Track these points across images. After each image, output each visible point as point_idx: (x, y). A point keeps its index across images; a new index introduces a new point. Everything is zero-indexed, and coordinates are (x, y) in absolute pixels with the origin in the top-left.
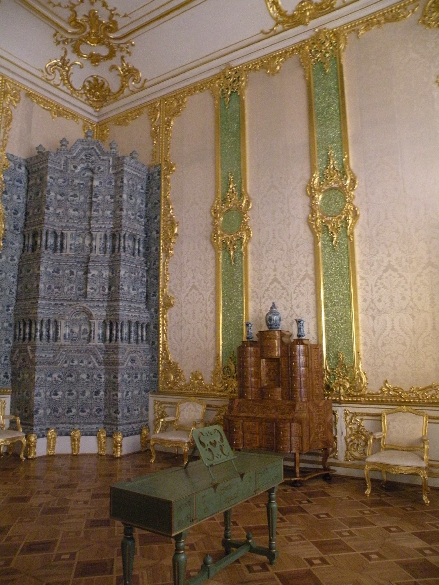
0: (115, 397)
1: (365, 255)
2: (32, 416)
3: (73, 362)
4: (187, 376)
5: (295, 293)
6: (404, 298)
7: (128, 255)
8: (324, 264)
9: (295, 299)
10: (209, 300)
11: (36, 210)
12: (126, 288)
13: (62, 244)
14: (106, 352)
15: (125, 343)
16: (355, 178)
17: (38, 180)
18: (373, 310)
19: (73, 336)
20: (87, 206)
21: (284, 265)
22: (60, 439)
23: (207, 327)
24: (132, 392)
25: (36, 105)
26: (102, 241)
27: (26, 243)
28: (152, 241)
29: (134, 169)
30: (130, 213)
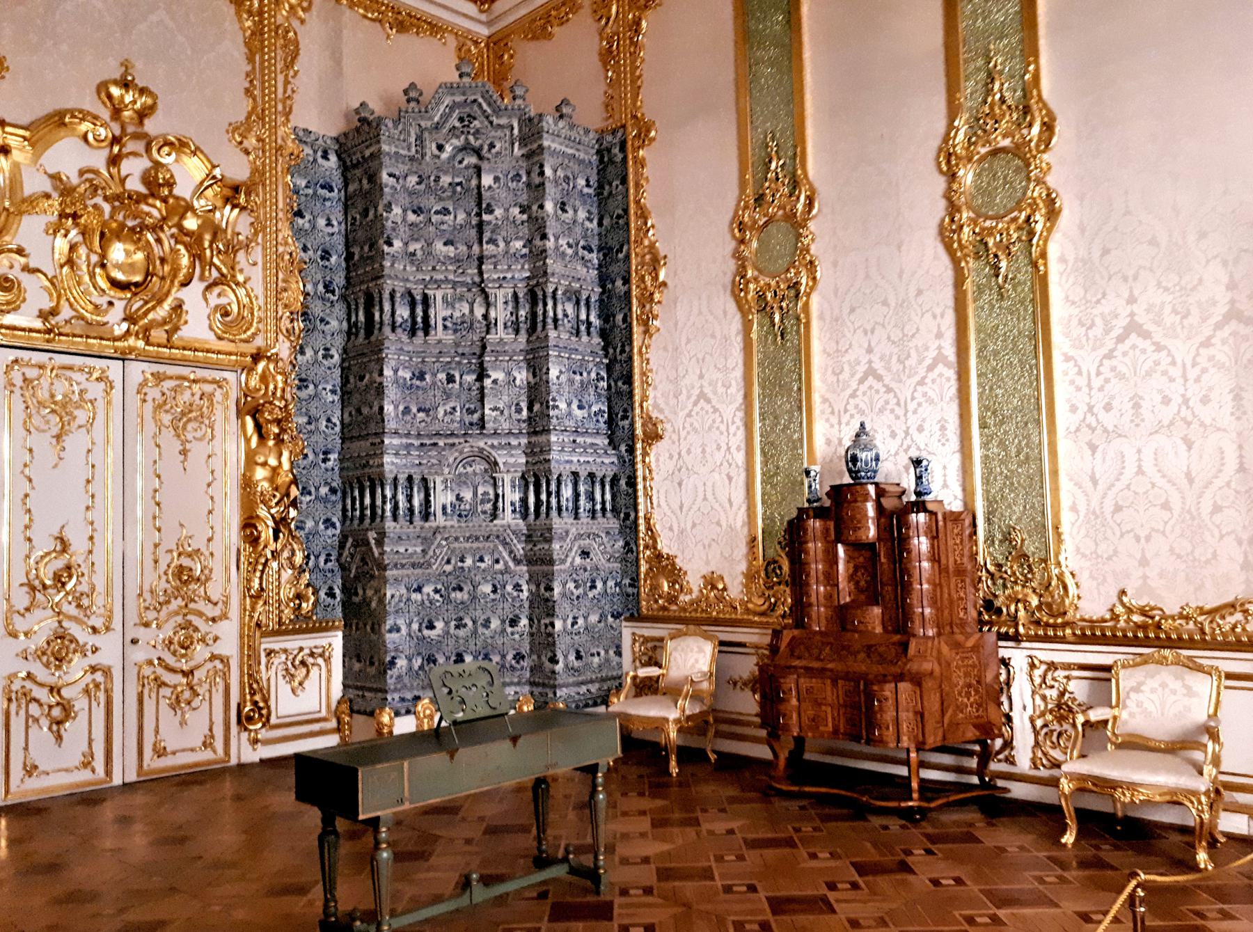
0: (550, 628)
1: (1073, 303)
2: (385, 672)
3: (462, 561)
4: (694, 582)
5: (913, 399)
6: (1166, 401)
7: (564, 336)
8: (978, 331)
9: (915, 412)
10: (733, 423)
11: (366, 248)
12: (563, 406)
13: (426, 318)
14: (529, 538)
15: (568, 519)
16: (1053, 118)
17: (365, 182)
18: (1094, 430)
19: (462, 507)
20: (474, 232)
21: (889, 338)
23: (730, 478)
24: (585, 618)
26: (510, 308)
27: (353, 319)
28: (614, 300)
30: (563, 242)
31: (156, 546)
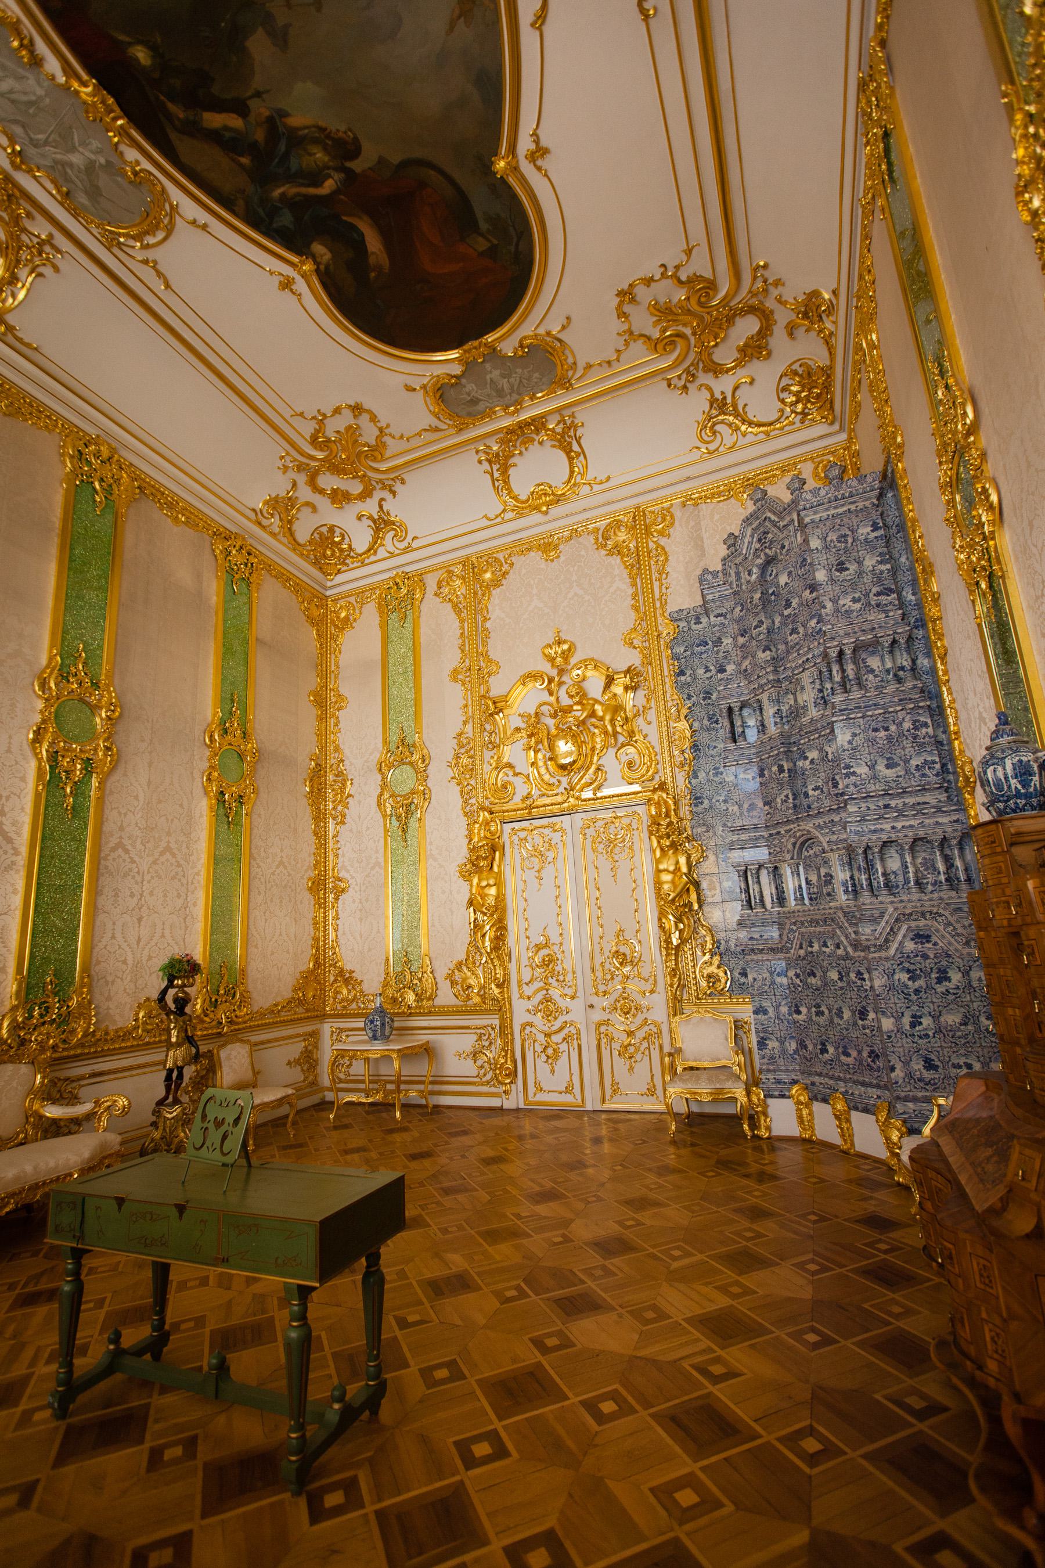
22: (817, 1106)
24: (936, 1018)
25: (704, 506)
29: (834, 504)
31: (601, 938)
